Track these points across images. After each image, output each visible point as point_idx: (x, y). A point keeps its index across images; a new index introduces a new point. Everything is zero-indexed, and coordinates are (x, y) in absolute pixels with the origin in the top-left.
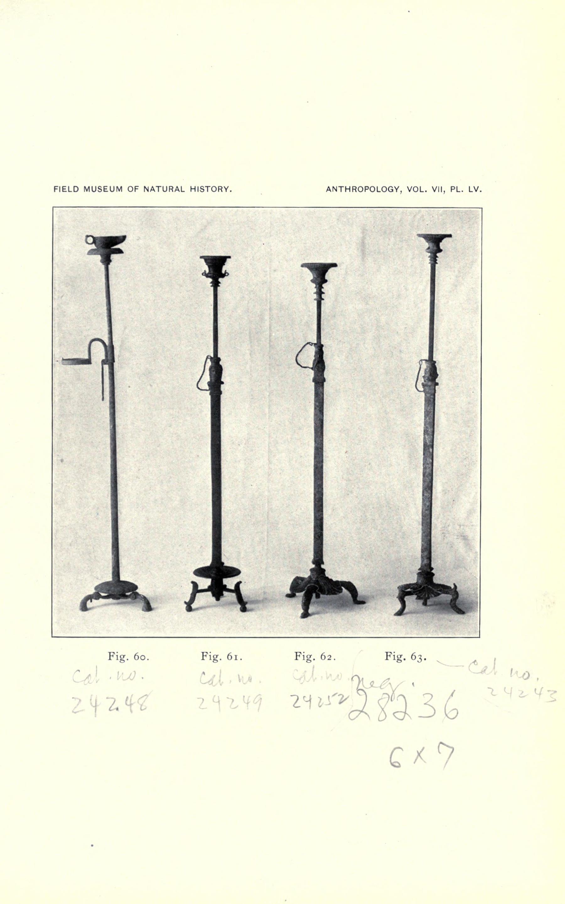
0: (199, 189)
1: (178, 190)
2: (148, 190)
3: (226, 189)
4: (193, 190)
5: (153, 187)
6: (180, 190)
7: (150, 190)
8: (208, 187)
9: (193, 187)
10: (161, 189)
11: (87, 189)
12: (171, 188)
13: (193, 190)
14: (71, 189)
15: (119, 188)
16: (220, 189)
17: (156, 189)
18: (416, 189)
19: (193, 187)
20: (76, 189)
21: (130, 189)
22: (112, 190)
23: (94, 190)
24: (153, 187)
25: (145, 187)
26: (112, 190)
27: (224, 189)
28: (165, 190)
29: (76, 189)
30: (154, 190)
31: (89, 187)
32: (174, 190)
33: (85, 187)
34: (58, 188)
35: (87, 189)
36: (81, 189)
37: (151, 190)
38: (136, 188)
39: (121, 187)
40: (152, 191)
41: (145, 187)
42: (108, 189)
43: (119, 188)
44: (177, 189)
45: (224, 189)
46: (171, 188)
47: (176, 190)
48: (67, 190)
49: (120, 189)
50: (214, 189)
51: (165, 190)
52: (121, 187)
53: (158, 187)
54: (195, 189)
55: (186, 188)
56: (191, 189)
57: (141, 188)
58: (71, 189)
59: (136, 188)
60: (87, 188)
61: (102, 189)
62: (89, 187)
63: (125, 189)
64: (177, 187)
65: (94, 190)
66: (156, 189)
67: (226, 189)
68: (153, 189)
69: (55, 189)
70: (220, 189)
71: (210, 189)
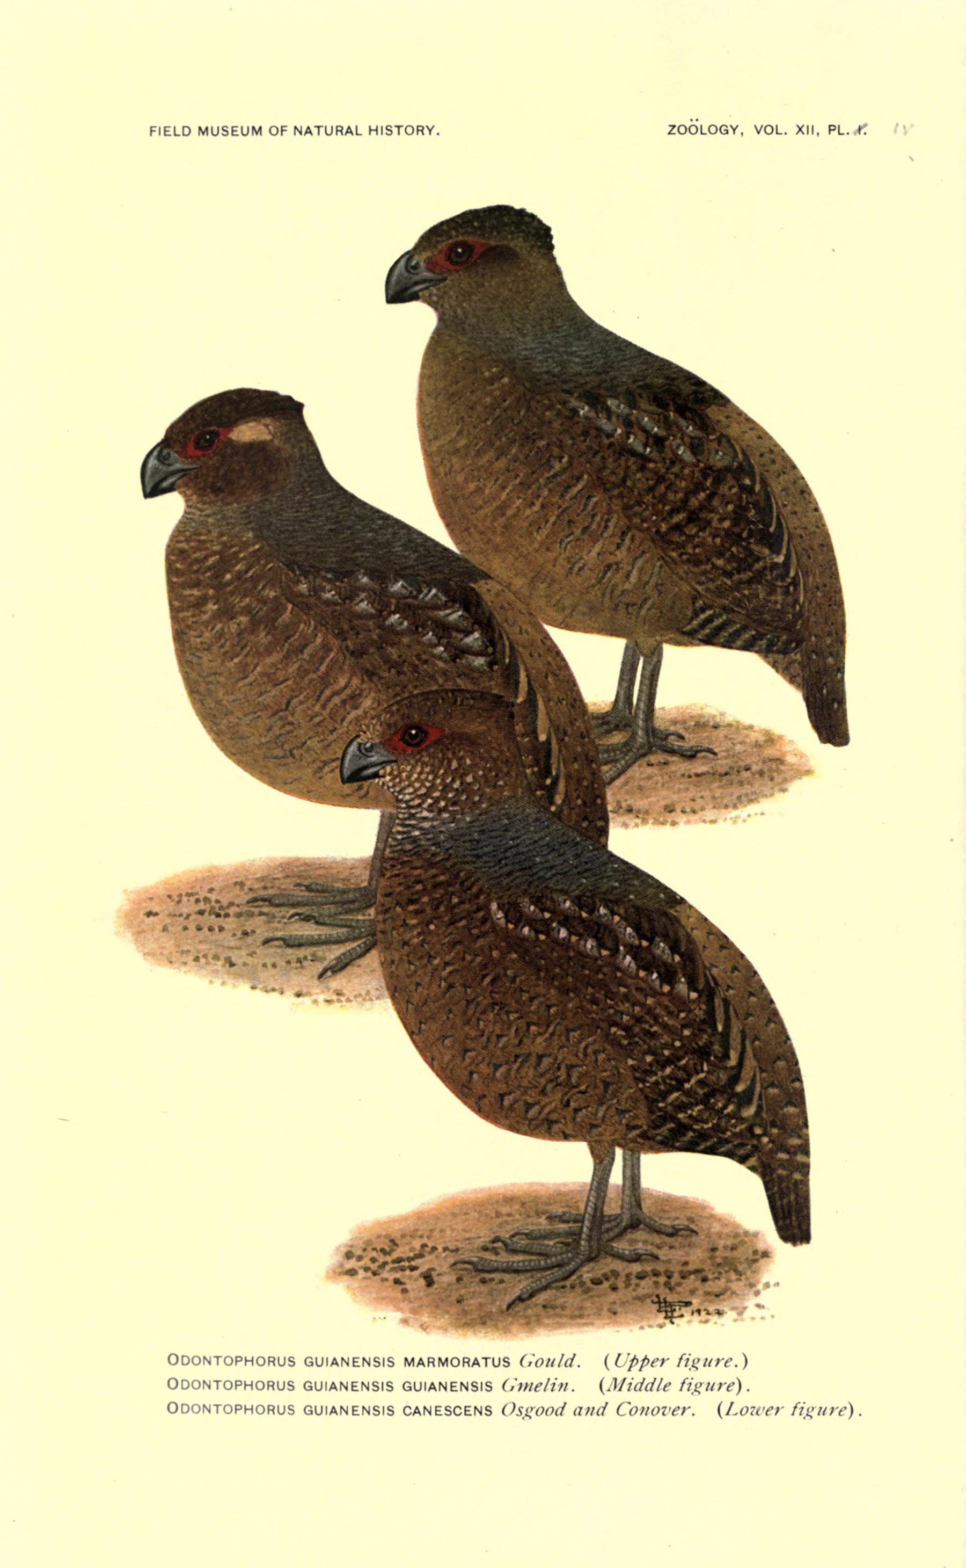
0: (385, 131)
1: (351, 132)
2: (301, 133)
3: (430, 131)
4: (373, 133)
5: (308, 128)
6: (354, 131)
7: (303, 132)
8: (399, 127)
9: (373, 127)
10: (322, 130)
11: (203, 131)
12: (339, 130)
13: (373, 133)
14: (179, 131)
15: (257, 129)
16: (420, 130)
17: (315, 131)
18: (769, 130)
19: (373, 127)
20: (186, 131)
21: (274, 131)
22: (245, 132)
23: (215, 132)
24: (308, 128)
25: (296, 128)
26: (245, 132)
27: (426, 131)
28: (329, 132)
29: (186, 131)
30: (310, 132)
31: (207, 129)
32: (344, 131)
33: (200, 128)
34: (157, 129)
35: (203, 131)
36: (195, 131)
37: (306, 132)
38: (283, 130)
39: (260, 128)
40: (309, 135)
41: (296, 128)
42: (239, 132)
43: (257, 129)
44: (349, 131)
45: (426, 131)
46: (339, 130)
47: (347, 132)
48: (172, 132)
49: (258, 131)
50: (409, 130)
51: (329, 132)
52: (260, 128)
53: (319, 127)
54: (376, 130)
55: (363, 130)
56: (370, 130)
57: (290, 130)
58: (179, 131)
59: (283, 130)
60: (203, 129)
61: (230, 131)
62: (207, 129)
63: (265, 131)
64: (349, 128)
65: (215, 132)
66: (315, 131)
67: (430, 131)
68: (309, 131)
69: (152, 131)
70: (420, 130)
71: (402, 130)
